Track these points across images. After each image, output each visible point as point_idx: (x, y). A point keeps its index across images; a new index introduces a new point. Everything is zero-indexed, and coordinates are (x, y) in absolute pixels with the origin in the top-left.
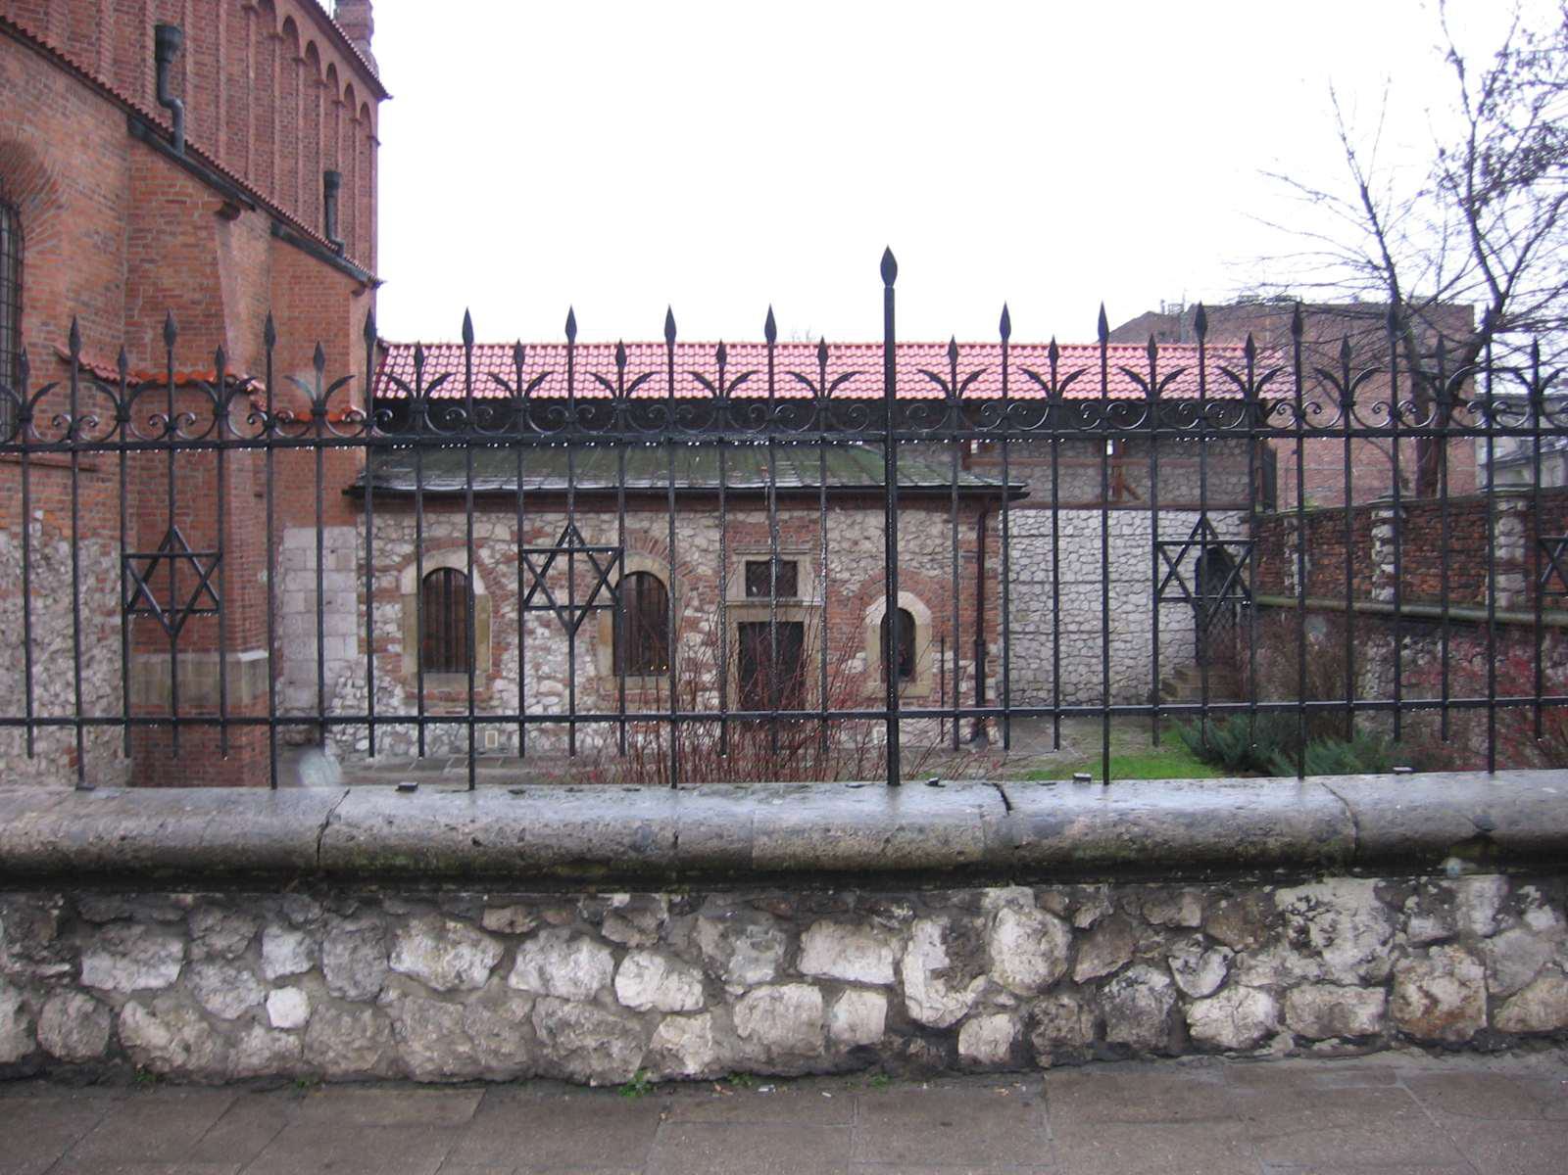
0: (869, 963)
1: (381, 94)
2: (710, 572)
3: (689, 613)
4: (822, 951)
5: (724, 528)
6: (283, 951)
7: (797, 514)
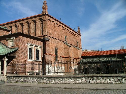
0: (79, 80)
1: (81, 36)
4: (78, 80)
6: (62, 79)
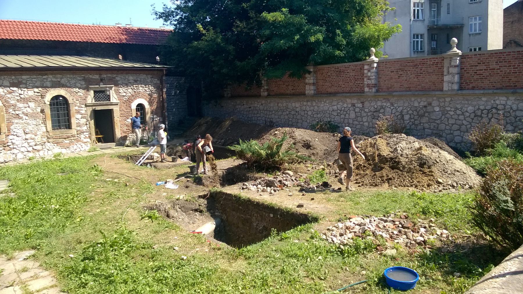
2: (82, 95)
3: (77, 108)
5: (84, 79)
7: (109, 75)
